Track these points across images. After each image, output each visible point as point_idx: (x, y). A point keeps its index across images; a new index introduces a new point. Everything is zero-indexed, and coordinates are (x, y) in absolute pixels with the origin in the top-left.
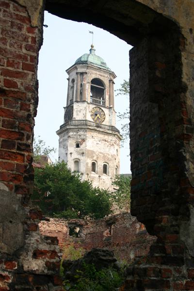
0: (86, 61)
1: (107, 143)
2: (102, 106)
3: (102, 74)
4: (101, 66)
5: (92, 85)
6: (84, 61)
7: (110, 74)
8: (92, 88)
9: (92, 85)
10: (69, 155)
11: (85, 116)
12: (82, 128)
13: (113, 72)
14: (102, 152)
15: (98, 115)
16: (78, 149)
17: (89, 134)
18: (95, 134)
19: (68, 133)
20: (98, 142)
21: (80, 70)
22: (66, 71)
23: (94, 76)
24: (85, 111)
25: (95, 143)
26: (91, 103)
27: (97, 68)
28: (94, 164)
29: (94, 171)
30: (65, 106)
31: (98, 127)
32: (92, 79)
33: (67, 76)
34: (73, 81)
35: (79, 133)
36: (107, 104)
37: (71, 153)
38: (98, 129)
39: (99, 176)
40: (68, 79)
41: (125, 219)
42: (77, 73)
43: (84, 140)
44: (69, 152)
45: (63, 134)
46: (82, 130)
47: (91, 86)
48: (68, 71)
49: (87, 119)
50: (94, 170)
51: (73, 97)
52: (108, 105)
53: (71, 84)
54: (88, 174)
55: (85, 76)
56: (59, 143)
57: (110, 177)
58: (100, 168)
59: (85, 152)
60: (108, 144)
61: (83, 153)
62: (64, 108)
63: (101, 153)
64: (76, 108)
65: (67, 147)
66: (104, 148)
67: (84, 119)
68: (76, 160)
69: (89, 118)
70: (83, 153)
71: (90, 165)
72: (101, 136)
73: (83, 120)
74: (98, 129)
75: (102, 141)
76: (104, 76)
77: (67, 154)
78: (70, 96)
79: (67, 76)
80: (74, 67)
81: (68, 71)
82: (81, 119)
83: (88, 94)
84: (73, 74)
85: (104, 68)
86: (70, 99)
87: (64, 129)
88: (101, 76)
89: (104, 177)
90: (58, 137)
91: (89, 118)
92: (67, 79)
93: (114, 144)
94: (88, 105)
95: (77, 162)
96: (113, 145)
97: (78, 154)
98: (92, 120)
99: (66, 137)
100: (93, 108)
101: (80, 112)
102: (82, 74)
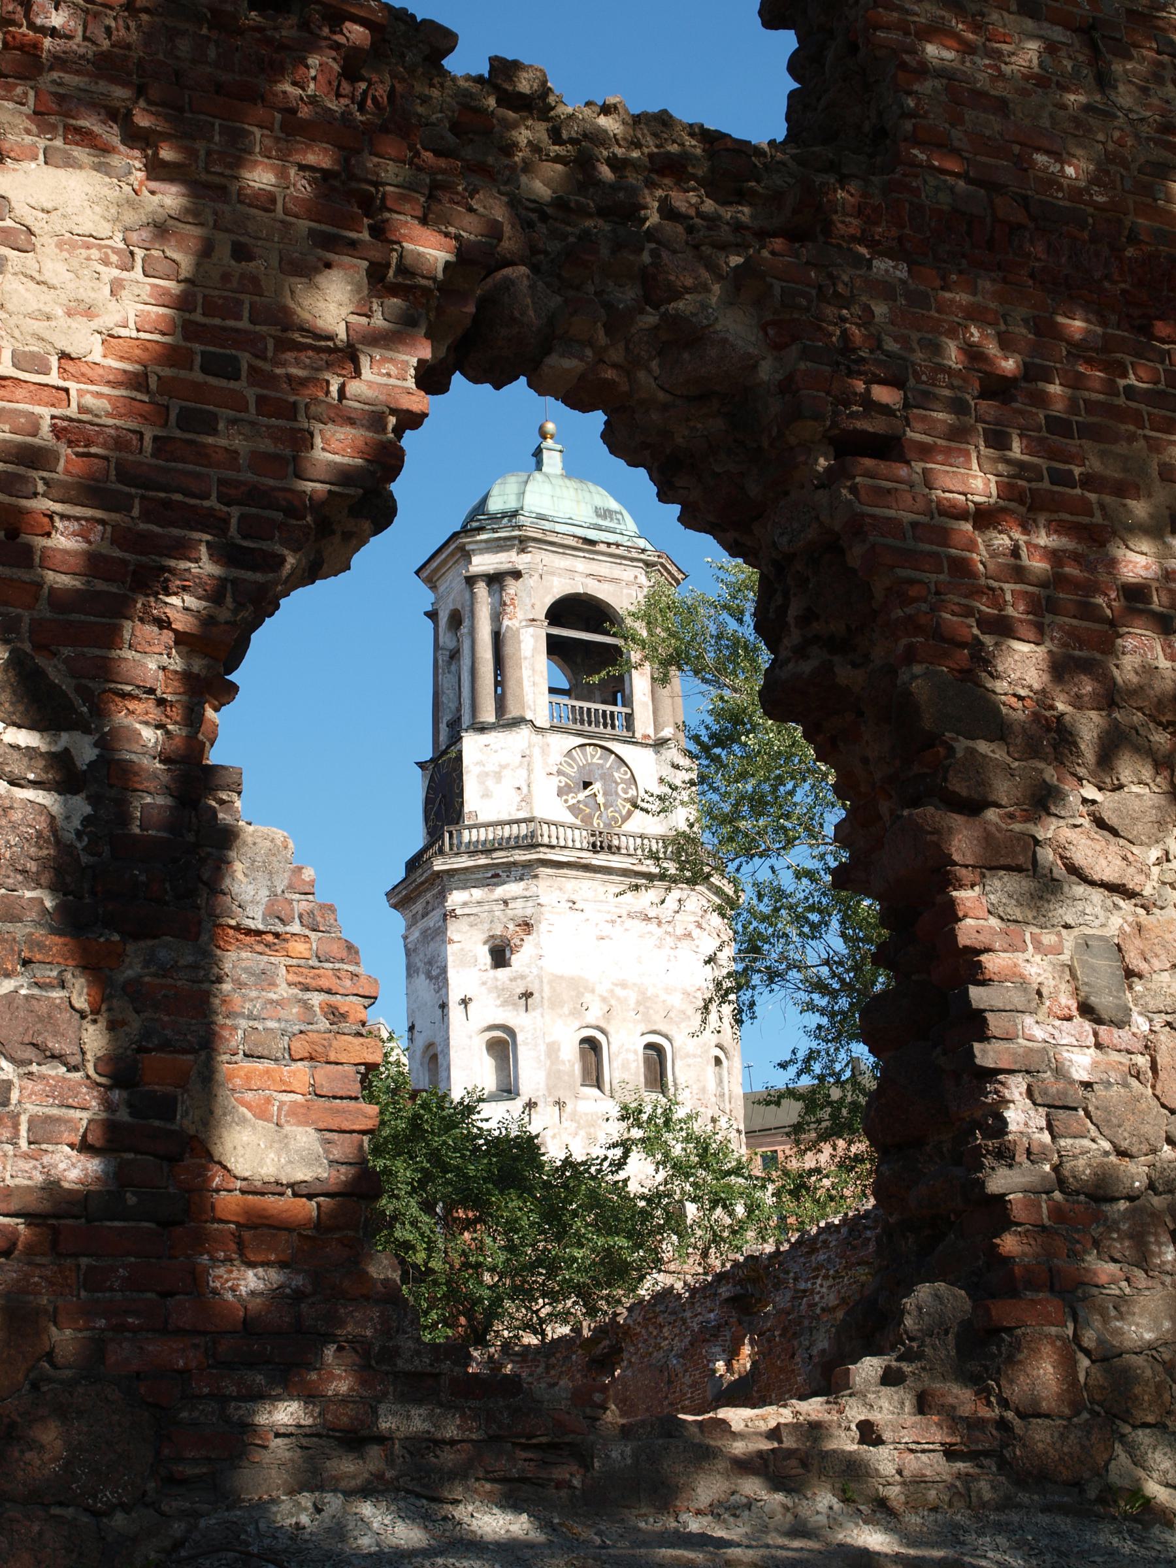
0: (515, 514)
2: (615, 739)
4: (599, 528)
5: (556, 631)
6: (505, 515)
7: (648, 564)
8: (555, 647)
9: (556, 631)
10: (455, 1012)
11: (527, 800)
12: (514, 864)
15: (597, 787)
16: (502, 973)
17: (550, 890)
19: (442, 896)
20: (607, 929)
21: (483, 563)
22: (417, 573)
23: (560, 587)
24: (524, 773)
26: (553, 728)
27: (571, 542)
28: (591, 1046)
29: (599, 1085)
30: (427, 755)
31: (595, 848)
32: (549, 601)
33: (426, 598)
34: (456, 620)
36: (644, 725)
37: (465, 1002)
38: (601, 860)
40: (432, 615)
41: (661, 1327)
42: (471, 581)
43: (527, 926)
44: (454, 997)
45: (418, 907)
47: (549, 637)
48: (429, 573)
49: (539, 813)
50: (594, 1076)
51: (459, 709)
52: (651, 731)
53: (446, 640)
55: (512, 587)
56: (408, 953)
58: (625, 1067)
59: (533, 988)
60: (659, 932)
61: (527, 995)
62: (421, 765)
64: (480, 763)
65: (444, 970)
67: (521, 815)
69: (550, 806)
70: (527, 995)
71: (570, 1053)
73: (517, 822)
74: (601, 860)
75: (629, 923)
76: (613, 580)
77: (444, 1006)
78: (444, 699)
79: (426, 598)
80: (455, 548)
81: (429, 573)
82: (505, 817)
83: (534, 674)
84: (452, 582)
85: (612, 538)
86: (446, 718)
87: (420, 877)
88: (600, 579)
90: (397, 921)
91: (550, 806)
92: (427, 614)
93: (696, 933)
94: (537, 738)
95: (502, 1047)
97: (505, 1003)
98: (569, 818)
99: (433, 920)
101: (498, 776)
102: (495, 580)
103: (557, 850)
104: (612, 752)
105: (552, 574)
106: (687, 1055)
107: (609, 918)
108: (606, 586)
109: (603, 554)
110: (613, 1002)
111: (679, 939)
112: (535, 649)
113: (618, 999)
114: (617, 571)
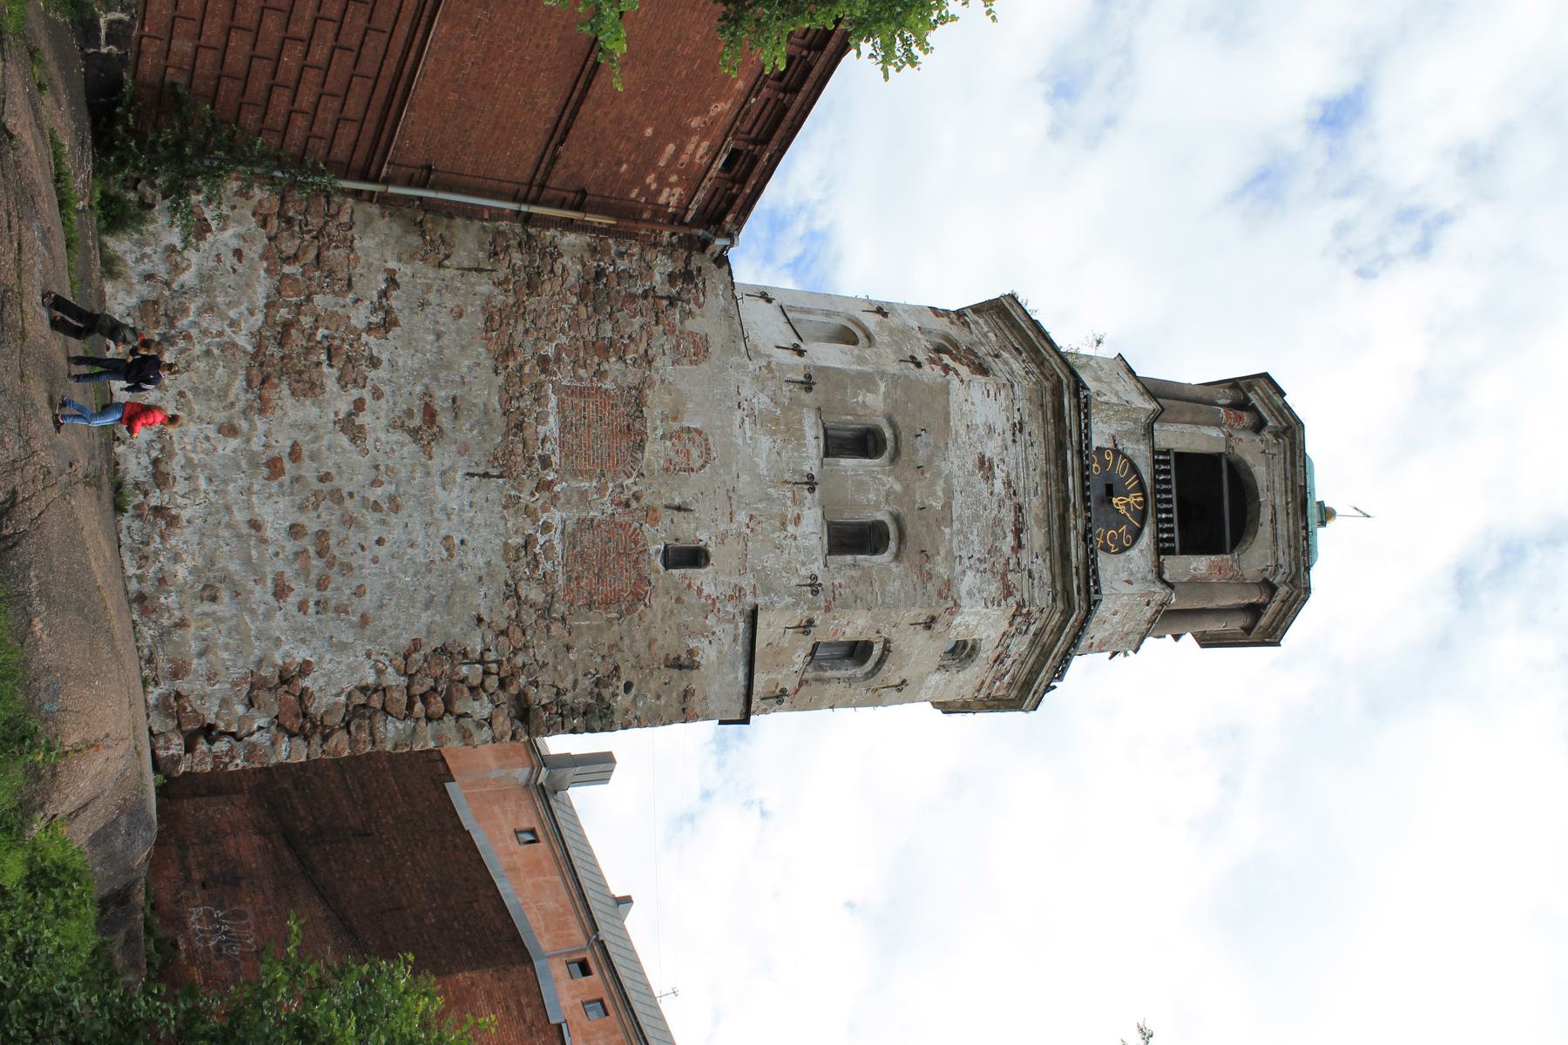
1: (1010, 538)
3: (1281, 517)
13: (1308, 590)
14: (958, 499)
18: (1038, 452)
23: (1260, 472)
25: (991, 449)
32: (1248, 459)
35: (1005, 355)
39: (811, 483)
43: (982, 370)
46: (1033, 367)
54: (808, 384)
57: (817, 568)
61: (919, 365)
63: (949, 494)
66: (976, 517)
68: (860, 334)
72: (1035, 506)
88: (1274, 521)
89: (811, 528)
96: (1008, 592)
100: (1134, 469)
103: (1074, 401)
104: (1143, 522)
105: (1268, 466)
106: (883, 583)
107: (1013, 477)
108: (1269, 529)
109: (1296, 524)
110: (928, 475)
111: (1004, 576)
112: (1210, 437)
113: (932, 484)
114: (1282, 544)
